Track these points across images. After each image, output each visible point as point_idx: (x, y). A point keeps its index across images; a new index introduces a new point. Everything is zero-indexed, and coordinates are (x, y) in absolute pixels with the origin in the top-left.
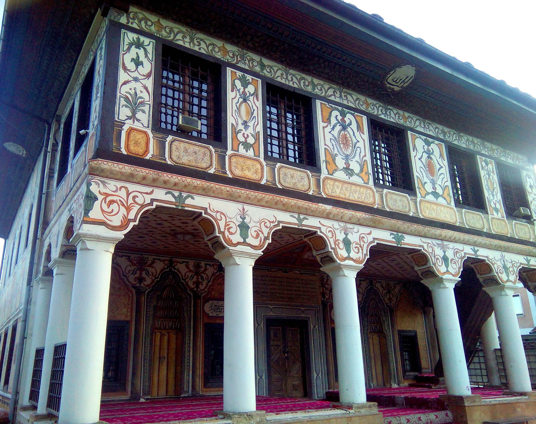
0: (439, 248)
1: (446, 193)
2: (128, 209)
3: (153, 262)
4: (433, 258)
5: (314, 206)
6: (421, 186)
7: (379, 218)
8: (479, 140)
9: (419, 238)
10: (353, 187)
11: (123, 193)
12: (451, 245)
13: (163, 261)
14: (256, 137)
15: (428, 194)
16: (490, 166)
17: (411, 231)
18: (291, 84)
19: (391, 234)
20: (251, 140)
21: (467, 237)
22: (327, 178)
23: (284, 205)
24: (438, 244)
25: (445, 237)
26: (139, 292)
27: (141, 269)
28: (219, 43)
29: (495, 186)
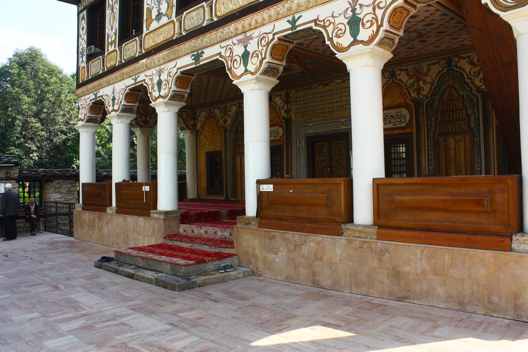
0: (240, 45)
3: (231, 107)
4: (229, 62)
9: (218, 45)
10: (161, 30)
12: (256, 33)
13: (236, 104)
17: (207, 42)
19: (192, 56)
24: (240, 41)
25: (243, 27)
26: (225, 131)
27: (225, 114)
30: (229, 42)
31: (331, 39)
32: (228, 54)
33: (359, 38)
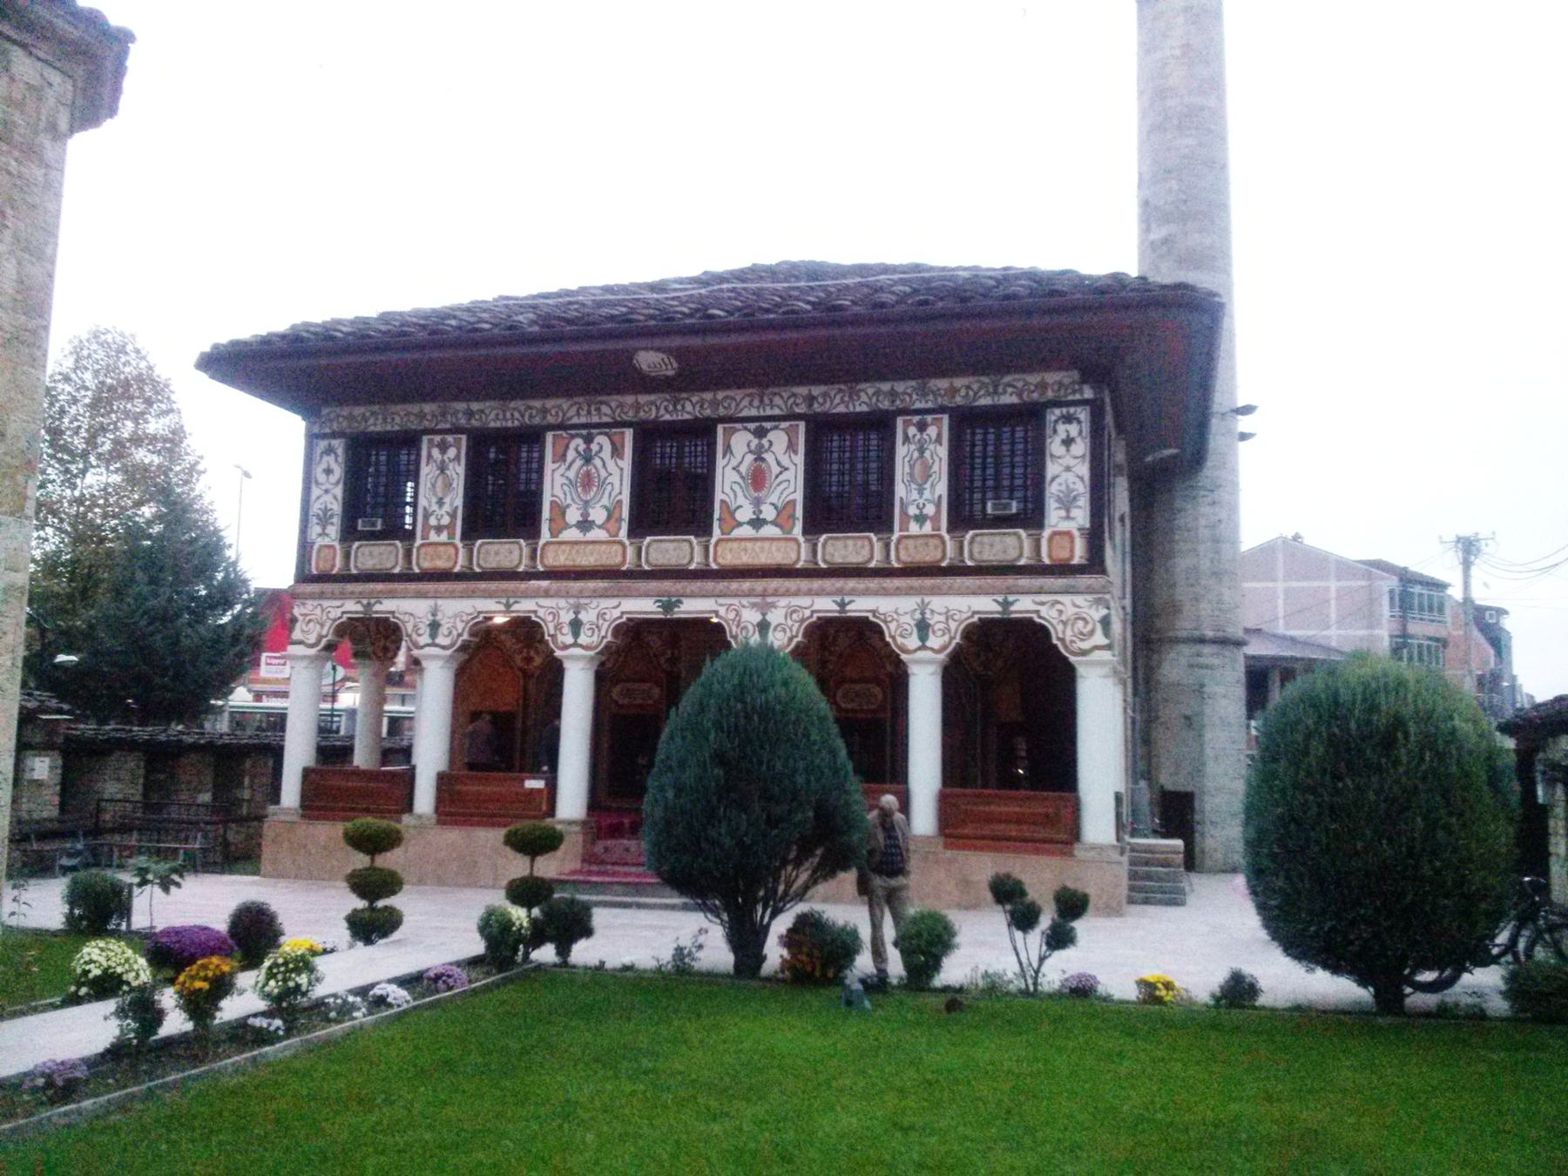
1: (785, 514)
2: (322, 625)
5: (523, 585)
6: (726, 516)
7: (625, 583)
8: (913, 383)
11: (318, 611)
12: (783, 602)
14: (453, 516)
15: (740, 524)
16: (932, 431)
18: (509, 424)
20: (446, 520)
21: (816, 584)
22: (547, 543)
23: (484, 591)
27: (529, 647)
28: (415, 408)
29: (936, 468)
30: (735, 601)
31: (893, 638)
32: (732, 615)
33: (928, 644)
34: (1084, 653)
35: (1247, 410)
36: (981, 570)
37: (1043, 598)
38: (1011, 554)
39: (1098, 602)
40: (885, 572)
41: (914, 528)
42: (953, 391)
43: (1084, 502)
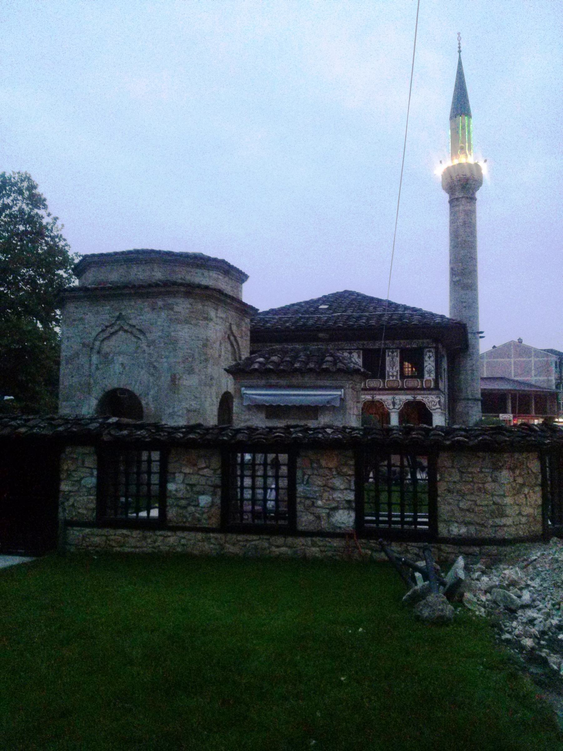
16: (395, 354)
21: (366, 392)
34: (434, 410)
35: (482, 332)
36: (409, 389)
37: (424, 396)
38: (416, 385)
39: (437, 397)
40: (384, 389)
41: (391, 378)
42: (400, 343)
43: (433, 372)
